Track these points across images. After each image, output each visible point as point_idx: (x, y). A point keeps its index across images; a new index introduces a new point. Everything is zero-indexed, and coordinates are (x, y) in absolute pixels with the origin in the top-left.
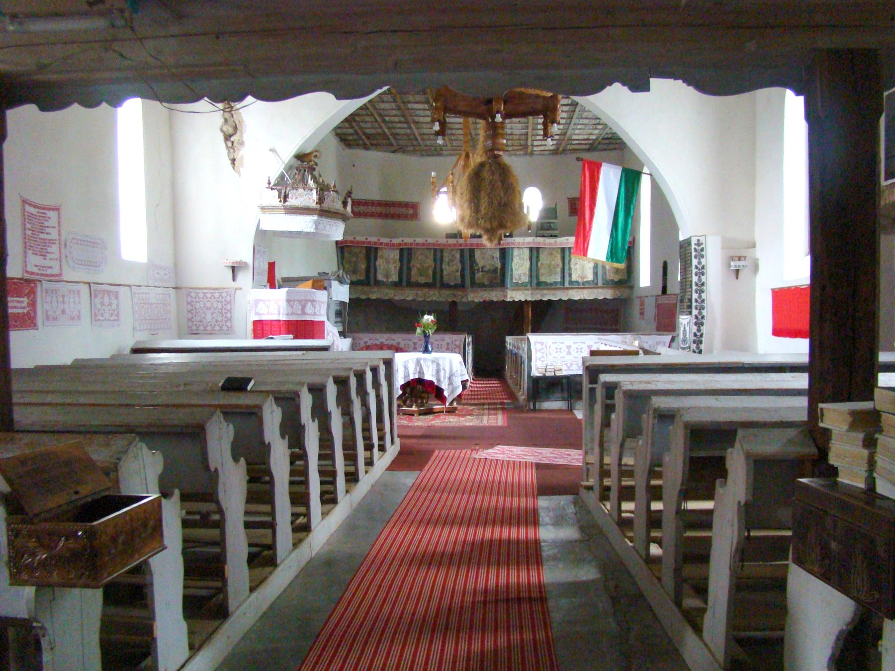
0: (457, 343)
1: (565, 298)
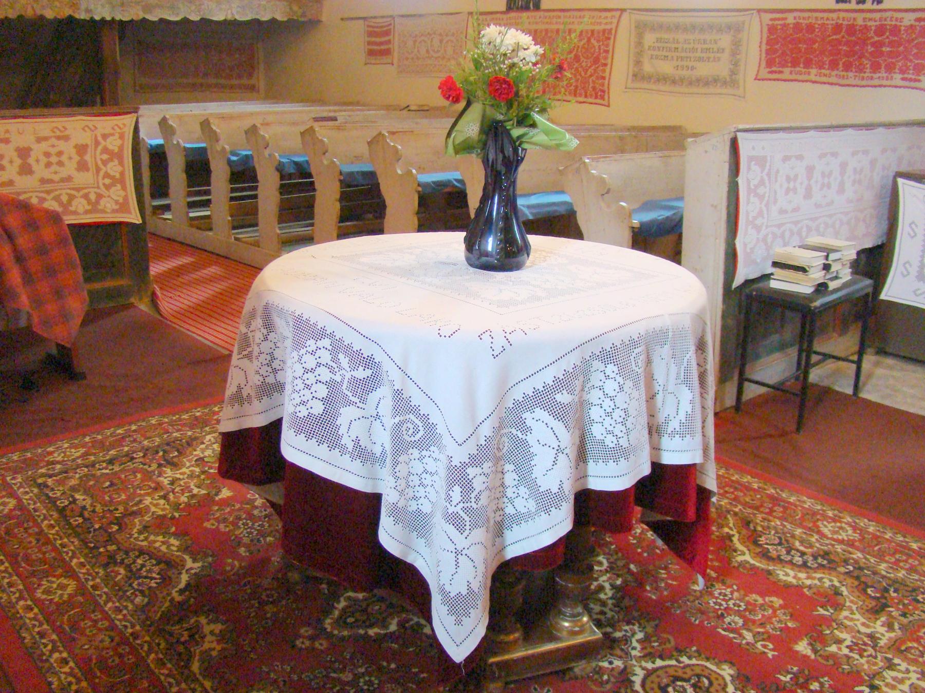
0: (113, 144)
1: (195, 18)
